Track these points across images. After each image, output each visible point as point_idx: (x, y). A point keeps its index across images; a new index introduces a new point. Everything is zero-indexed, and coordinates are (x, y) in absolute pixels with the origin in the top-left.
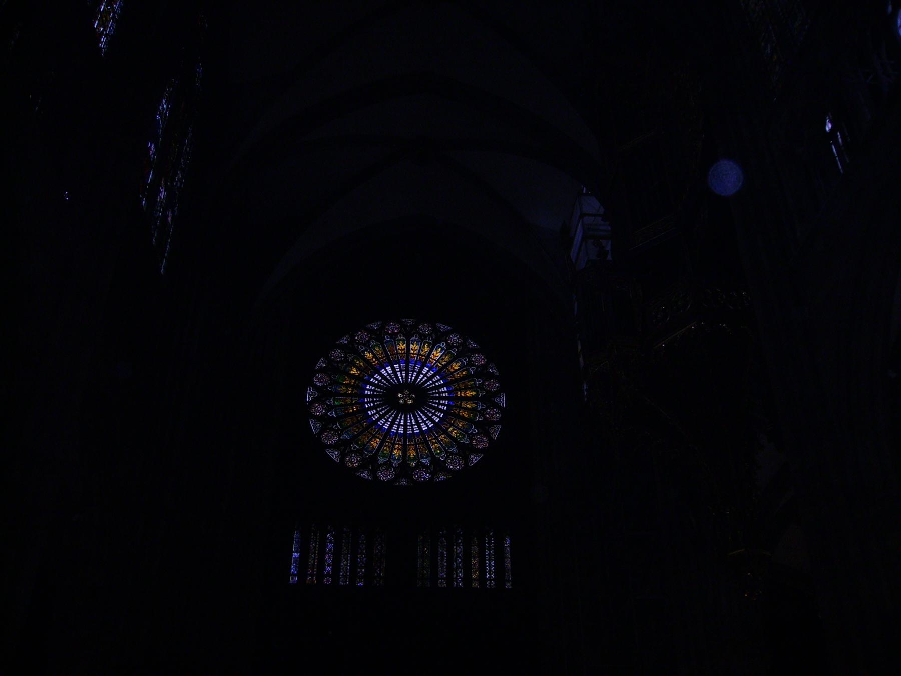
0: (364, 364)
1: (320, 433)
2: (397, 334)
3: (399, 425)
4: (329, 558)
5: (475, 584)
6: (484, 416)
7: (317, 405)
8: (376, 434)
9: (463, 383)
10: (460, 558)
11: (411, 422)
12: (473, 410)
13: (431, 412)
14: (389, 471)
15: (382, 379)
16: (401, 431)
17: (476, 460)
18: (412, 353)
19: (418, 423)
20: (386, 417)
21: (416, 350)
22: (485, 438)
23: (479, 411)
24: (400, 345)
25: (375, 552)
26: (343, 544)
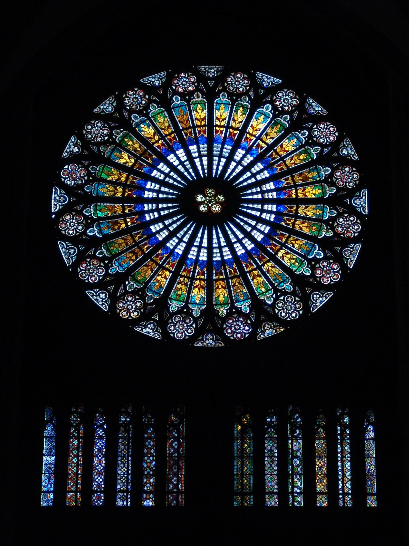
0: (140, 146)
1: (76, 264)
2: (191, 94)
3: (200, 247)
4: (100, 461)
5: (321, 499)
6: (333, 228)
7: (68, 217)
8: (163, 263)
9: (300, 175)
10: (297, 457)
11: (219, 243)
12: (319, 220)
13: (250, 225)
14: (187, 323)
15: (170, 172)
16: (203, 256)
17: (321, 303)
18: (217, 126)
19: (230, 245)
20: (178, 235)
21: (223, 120)
22: (335, 267)
23: (326, 222)
24: (197, 111)
25: (168, 452)
26: (120, 441)
